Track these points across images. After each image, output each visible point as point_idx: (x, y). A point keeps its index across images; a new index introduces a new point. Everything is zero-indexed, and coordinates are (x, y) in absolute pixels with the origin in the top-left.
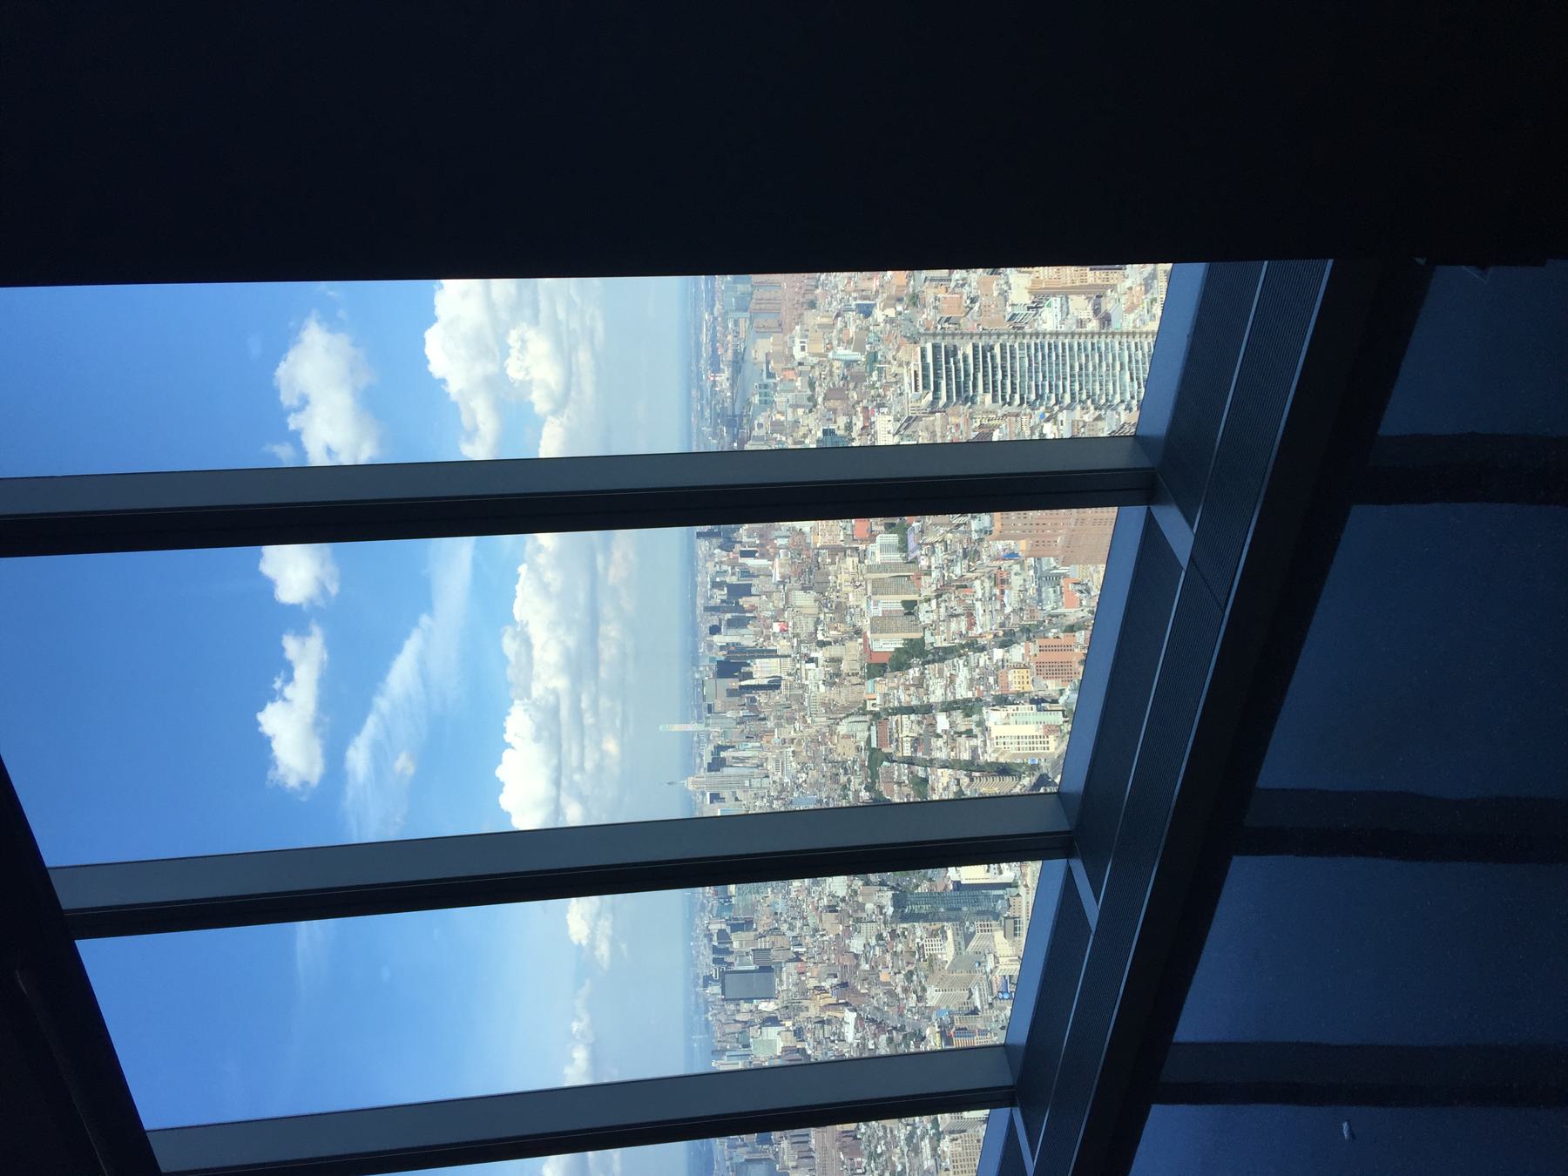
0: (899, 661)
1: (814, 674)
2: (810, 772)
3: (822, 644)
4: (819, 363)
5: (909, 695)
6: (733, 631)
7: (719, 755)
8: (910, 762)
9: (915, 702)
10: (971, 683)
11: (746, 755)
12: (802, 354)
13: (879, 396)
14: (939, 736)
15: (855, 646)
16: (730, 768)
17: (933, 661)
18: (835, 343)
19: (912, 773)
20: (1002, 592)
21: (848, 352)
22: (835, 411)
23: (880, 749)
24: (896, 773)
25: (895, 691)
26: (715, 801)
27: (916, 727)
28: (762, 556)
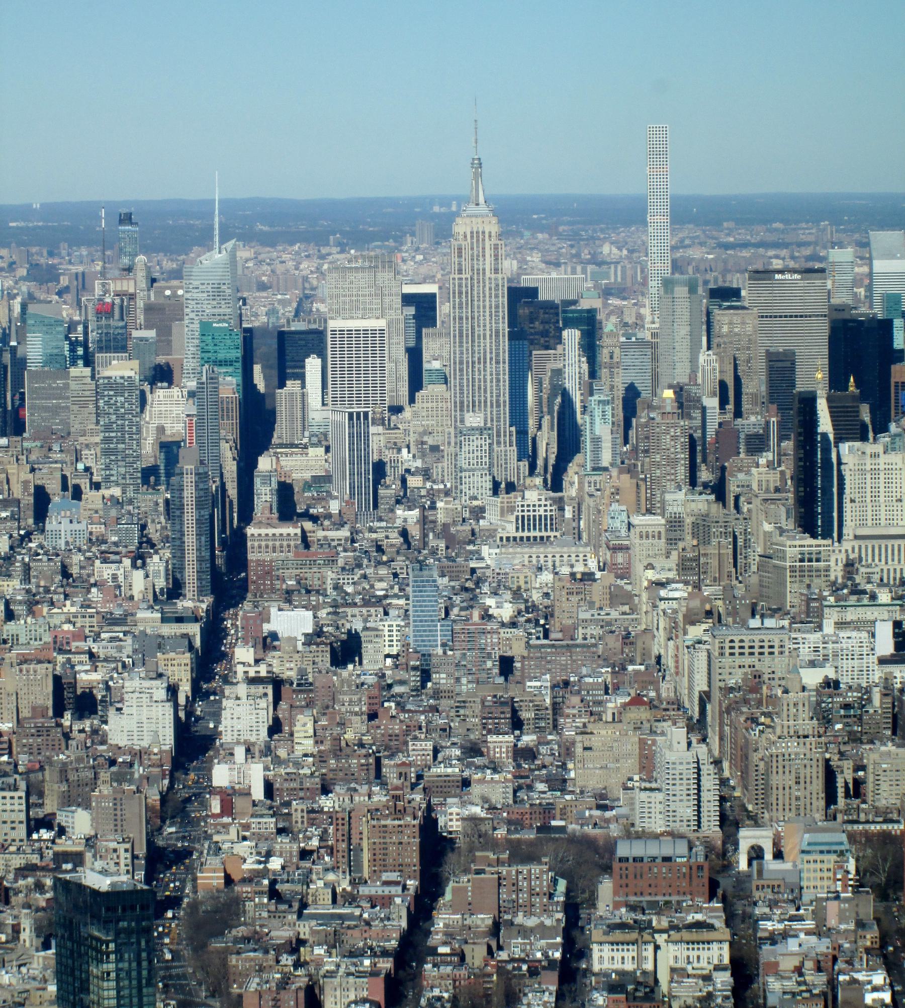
2: (520, 632)
5: (799, 970)
7: (569, 323)
19: (533, 972)
23: (607, 869)
24: (532, 922)
25: (810, 924)
26: (411, 311)
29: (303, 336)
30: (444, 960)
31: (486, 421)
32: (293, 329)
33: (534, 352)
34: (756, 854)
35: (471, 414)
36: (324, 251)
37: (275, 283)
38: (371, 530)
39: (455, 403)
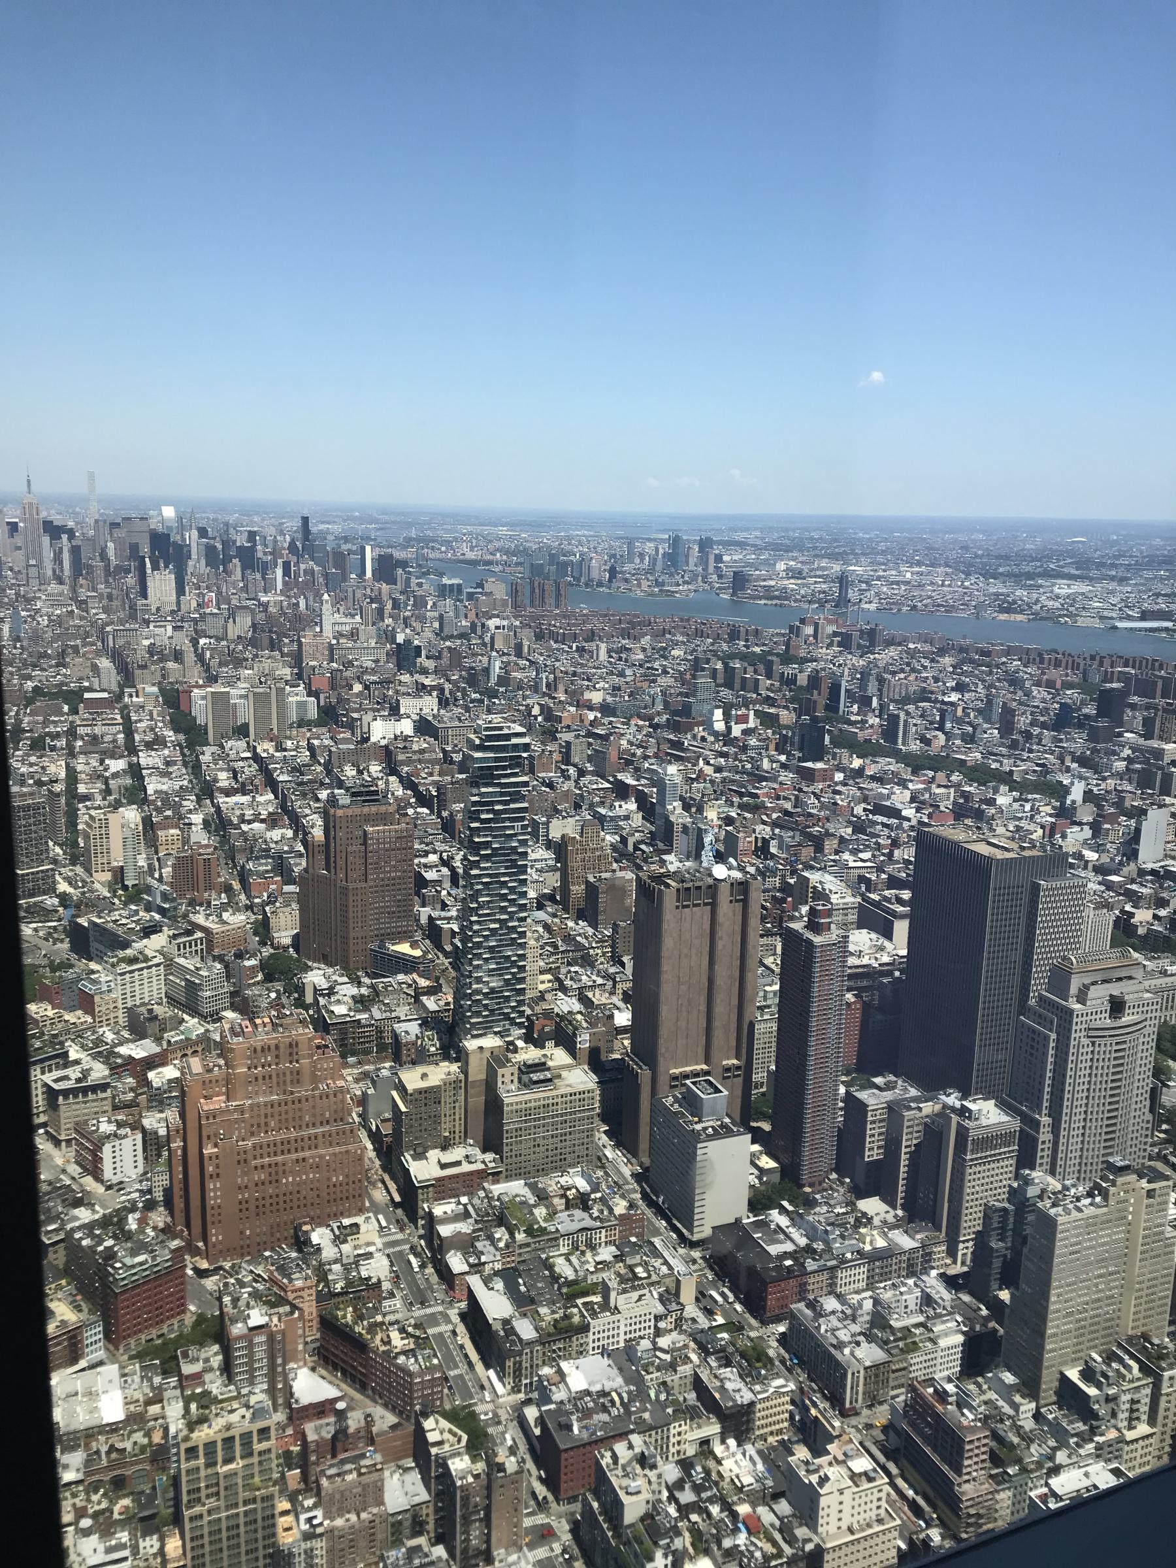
0: (183, 721)
1: (164, 634)
3: (195, 642)
4: (484, 644)
6: (202, 548)
8: (72, 733)
9: (137, 737)
10: (163, 796)
12: (492, 627)
13: (456, 700)
14: (102, 762)
15: (195, 675)
17: (183, 755)
18: (505, 659)
20: (263, 821)
21: (497, 670)
22: (439, 657)
27: (108, 738)
28: (285, 583)
30: (27, 731)
34: (131, 696)
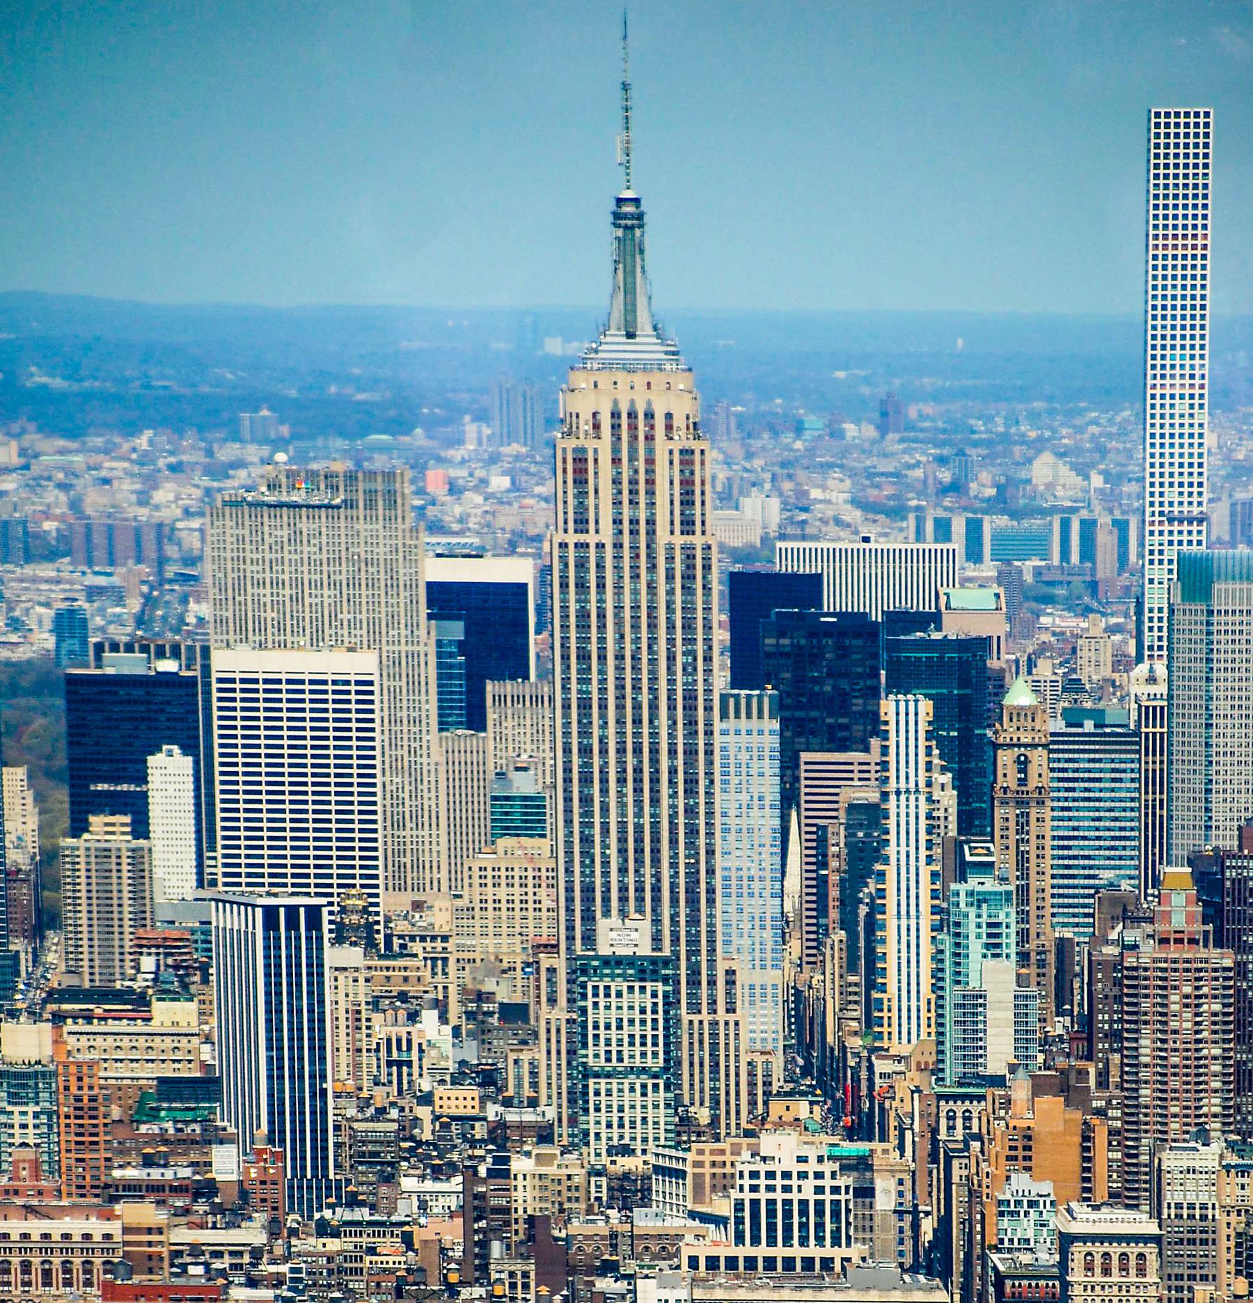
11: (891, 948)
16: (770, 787)
26: (456, 630)
29: (138, 693)
31: (657, 939)
32: (110, 671)
33: (805, 756)
35: (615, 920)
36: (227, 453)
37: (78, 542)
38: (324, 1229)
39: (569, 889)
